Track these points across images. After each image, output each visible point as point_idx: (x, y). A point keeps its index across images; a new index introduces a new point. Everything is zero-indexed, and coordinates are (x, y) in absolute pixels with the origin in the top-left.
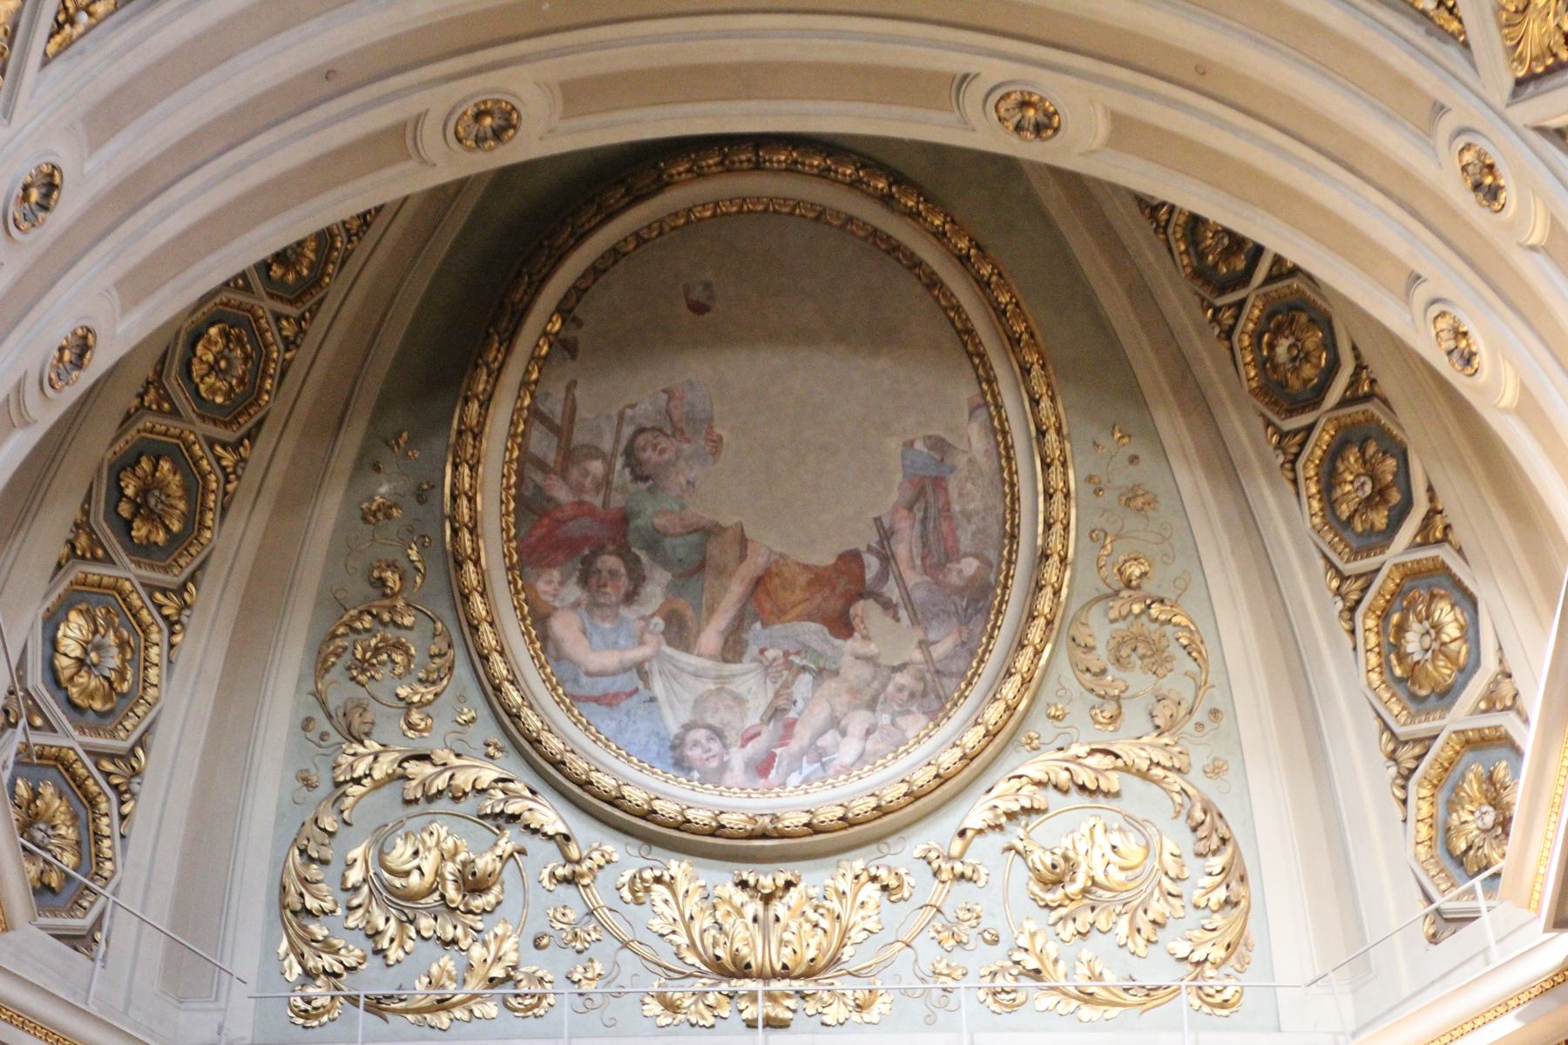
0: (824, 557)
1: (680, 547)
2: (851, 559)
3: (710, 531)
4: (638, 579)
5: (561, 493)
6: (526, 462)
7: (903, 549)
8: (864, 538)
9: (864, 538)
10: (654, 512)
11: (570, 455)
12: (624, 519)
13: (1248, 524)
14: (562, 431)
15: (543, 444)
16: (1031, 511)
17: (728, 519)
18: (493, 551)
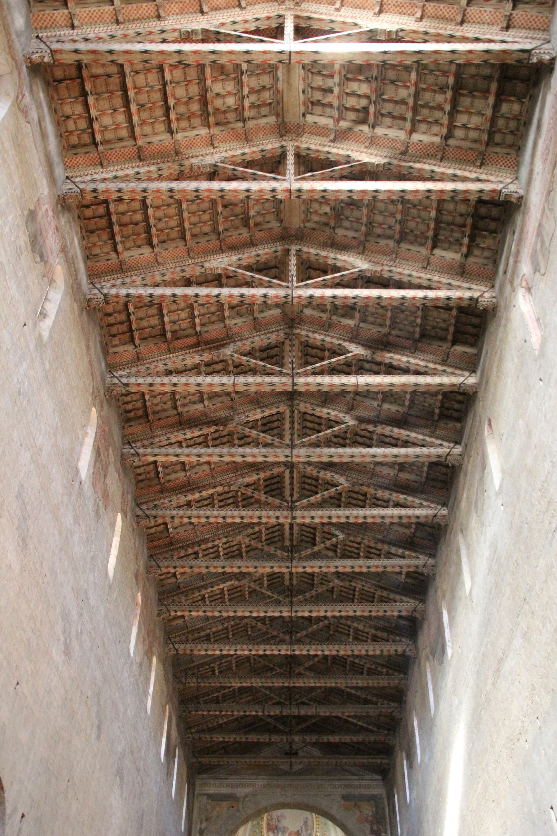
0: (296, 831)
1: (282, 829)
2: (298, 831)
3: (285, 827)
4: (278, 833)
5: (271, 823)
6: (268, 820)
7: (303, 829)
8: (299, 828)
9: (299, 828)
10: (280, 825)
11: (272, 819)
12: (277, 826)
13: (335, 830)
14: (271, 816)
15: (269, 818)
16: (315, 826)
17: (286, 826)
18: (265, 831)
